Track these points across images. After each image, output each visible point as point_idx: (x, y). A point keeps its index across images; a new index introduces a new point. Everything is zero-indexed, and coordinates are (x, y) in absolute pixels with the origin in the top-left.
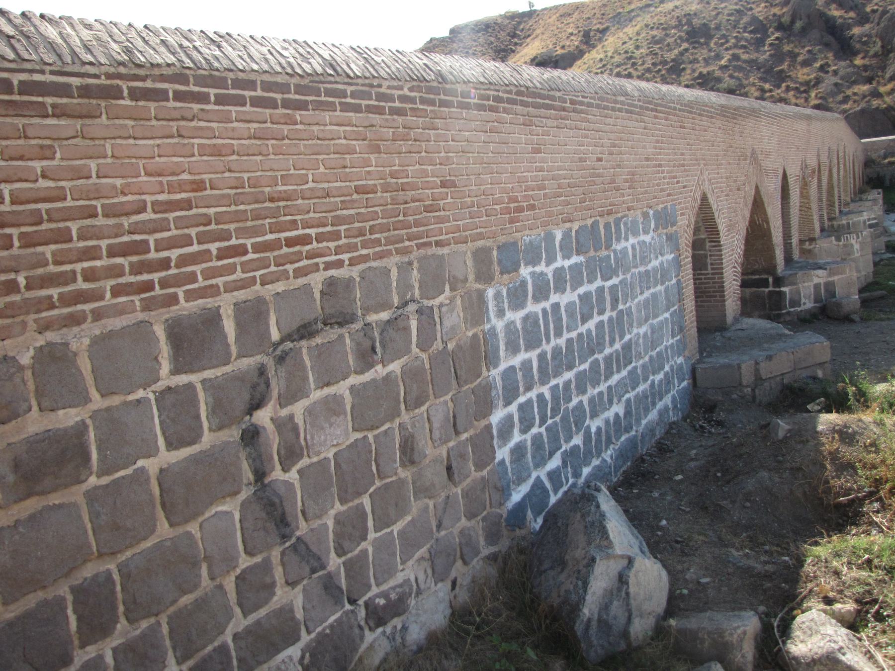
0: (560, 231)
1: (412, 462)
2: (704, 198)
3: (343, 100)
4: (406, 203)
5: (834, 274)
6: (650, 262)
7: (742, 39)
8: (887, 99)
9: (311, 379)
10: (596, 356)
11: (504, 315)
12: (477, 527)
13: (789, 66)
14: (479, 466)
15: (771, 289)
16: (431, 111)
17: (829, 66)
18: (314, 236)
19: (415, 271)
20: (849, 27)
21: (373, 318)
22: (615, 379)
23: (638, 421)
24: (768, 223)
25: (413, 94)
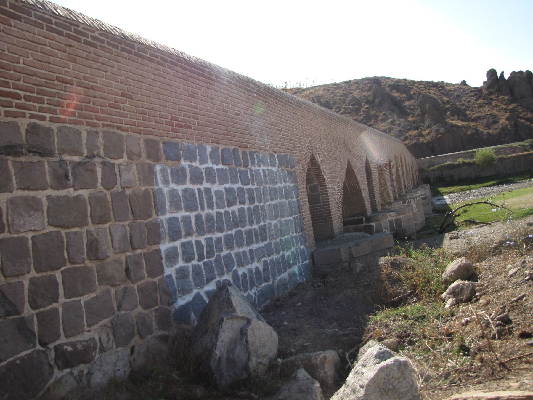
0: (210, 147)
1: (98, 259)
2: (313, 160)
3: (49, 25)
4: (95, 97)
6: (277, 183)
7: (348, 108)
8: (427, 138)
9: (14, 181)
10: (239, 228)
11: (169, 184)
12: (151, 314)
13: (375, 122)
14: (152, 274)
15: (365, 224)
16: (115, 51)
17: (395, 121)
18: (22, 96)
19: (101, 139)
20: (403, 102)
21: (67, 157)
22: (254, 246)
23: (274, 276)
24: (358, 185)
25: (102, 38)
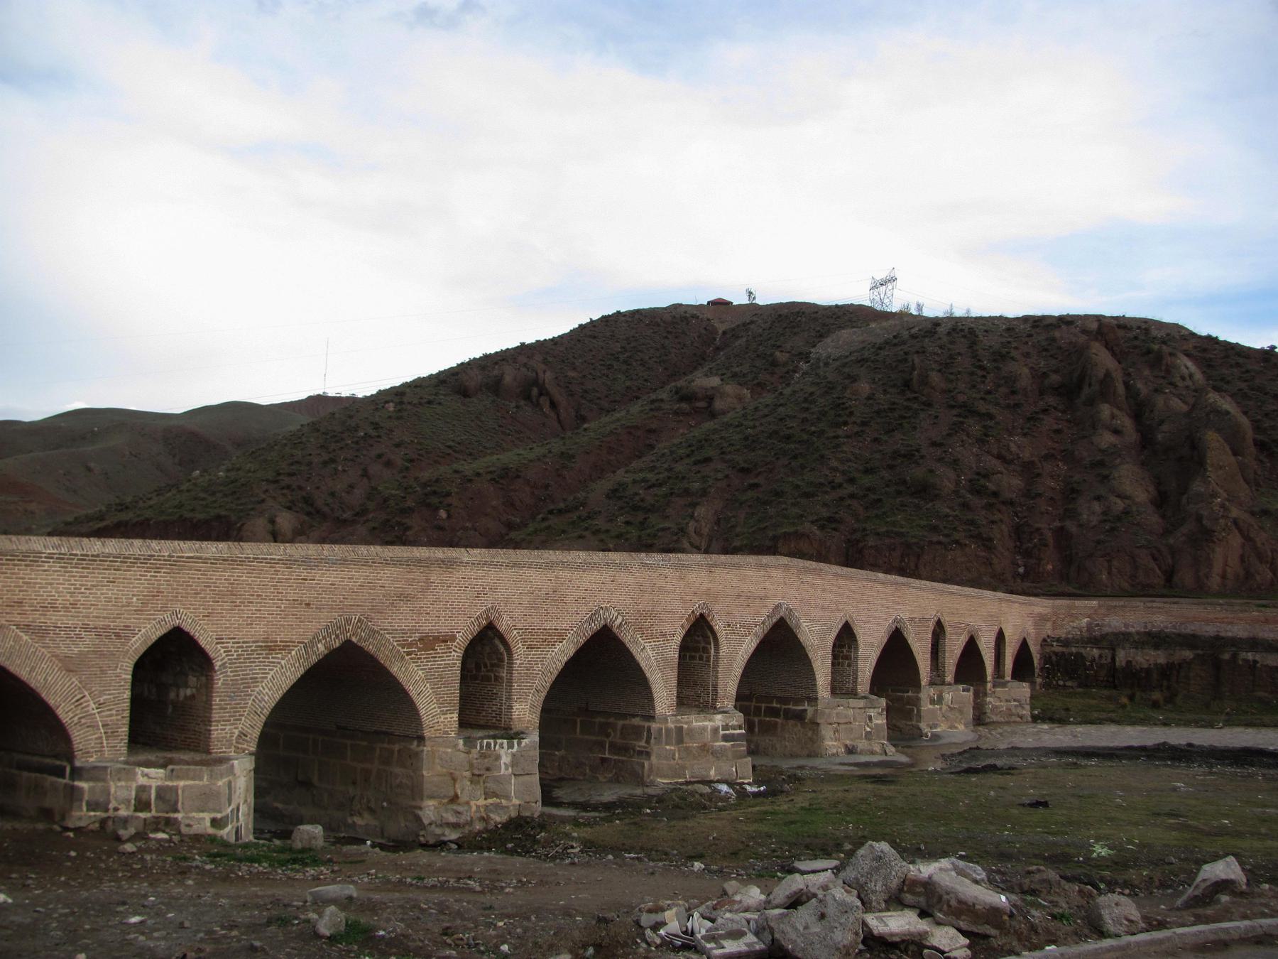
5: (179, 778)
